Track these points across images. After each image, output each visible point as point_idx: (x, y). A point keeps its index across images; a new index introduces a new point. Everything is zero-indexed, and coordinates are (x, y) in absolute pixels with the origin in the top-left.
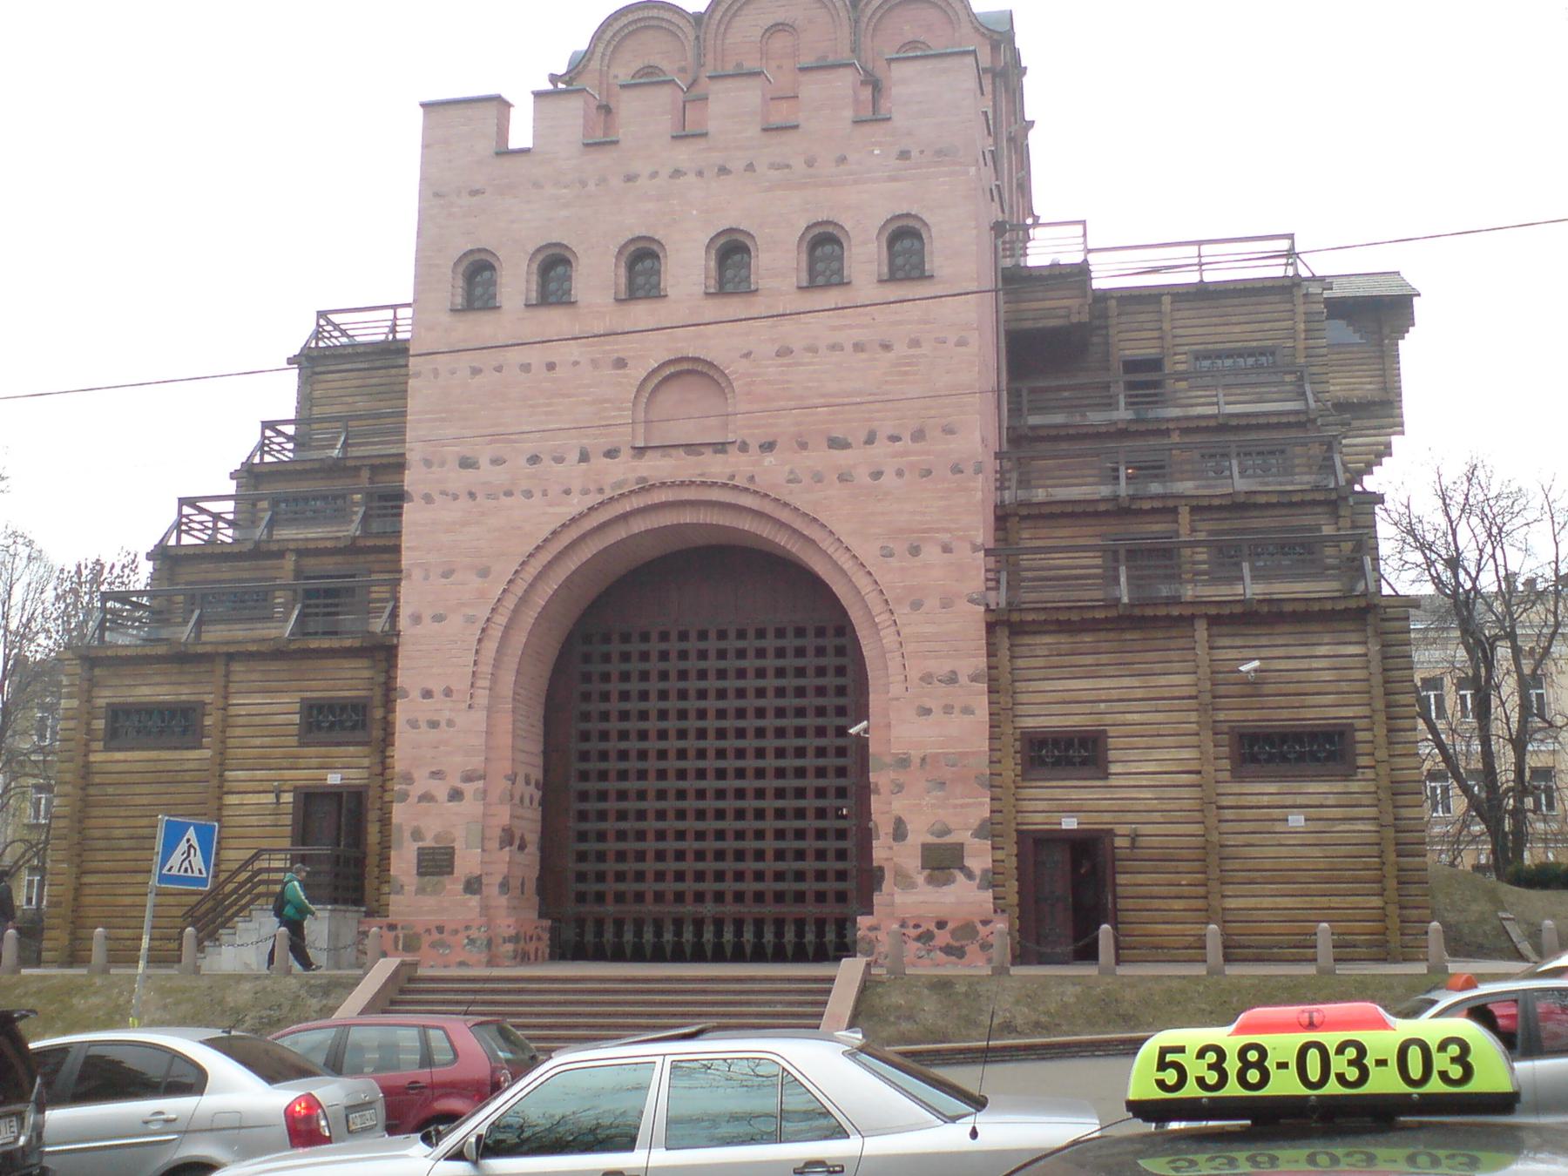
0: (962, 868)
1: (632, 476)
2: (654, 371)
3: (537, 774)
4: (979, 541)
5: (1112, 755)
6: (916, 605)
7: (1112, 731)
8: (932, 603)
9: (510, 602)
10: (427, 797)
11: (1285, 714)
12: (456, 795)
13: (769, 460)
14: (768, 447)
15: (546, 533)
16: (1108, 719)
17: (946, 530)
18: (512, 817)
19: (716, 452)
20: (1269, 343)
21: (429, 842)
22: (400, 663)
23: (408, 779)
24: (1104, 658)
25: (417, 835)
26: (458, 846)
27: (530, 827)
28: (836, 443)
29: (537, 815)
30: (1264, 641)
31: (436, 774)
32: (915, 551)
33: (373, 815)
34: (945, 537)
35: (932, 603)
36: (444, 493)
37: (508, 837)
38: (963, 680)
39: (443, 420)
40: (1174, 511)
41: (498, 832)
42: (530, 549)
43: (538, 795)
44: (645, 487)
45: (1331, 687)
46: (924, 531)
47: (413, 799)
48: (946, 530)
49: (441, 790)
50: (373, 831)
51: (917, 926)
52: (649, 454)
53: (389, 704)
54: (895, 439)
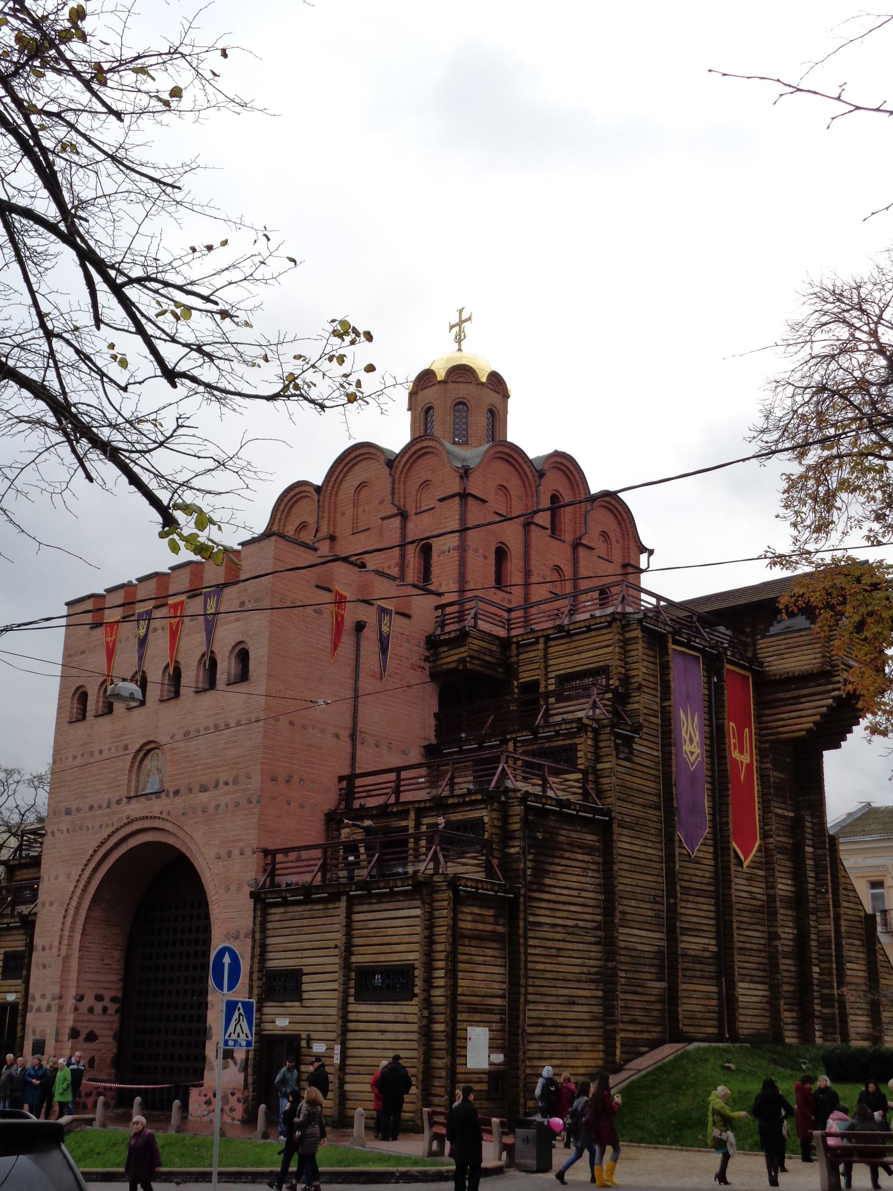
0: (233, 1058)
1: (124, 815)
2: (139, 751)
3: (119, 994)
4: (255, 846)
5: (305, 987)
6: (228, 889)
7: (306, 970)
8: (234, 888)
9: (79, 891)
10: (39, 1010)
11: (382, 958)
12: (49, 1008)
13: (177, 800)
14: (177, 793)
15: (91, 852)
16: (304, 961)
17: (242, 840)
18: (75, 1021)
19: (157, 798)
20: (602, 664)
21: (38, 1037)
22: (37, 930)
23: (34, 1000)
24: (305, 922)
25: (34, 1033)
26: (48, 1038)
27: (106, 1028)
28: (204, 789)
29: (116, 1018)
30: (376, 907)
31: (43, 996)
32: (229, 854)
33: (19, 1020)
34: (242, 844)
35: (234, 888)
36: (58, 830)
37: (74, 1034)
38: (242, 936)
39: (60, 787)
40: (407, 812)
41: (67, 1031)
42: (85, 861)
43: (113, 1007)
44: (131, 822)
45: (406, 939)
46: (235, 841)
47: (34, 1010)
48: (242, 840)
49: (43, 1004)
50: (19, 1028)
51: (205, 1095)
52: (134, 801)
53: (31, 956)
54: (226, 784)
